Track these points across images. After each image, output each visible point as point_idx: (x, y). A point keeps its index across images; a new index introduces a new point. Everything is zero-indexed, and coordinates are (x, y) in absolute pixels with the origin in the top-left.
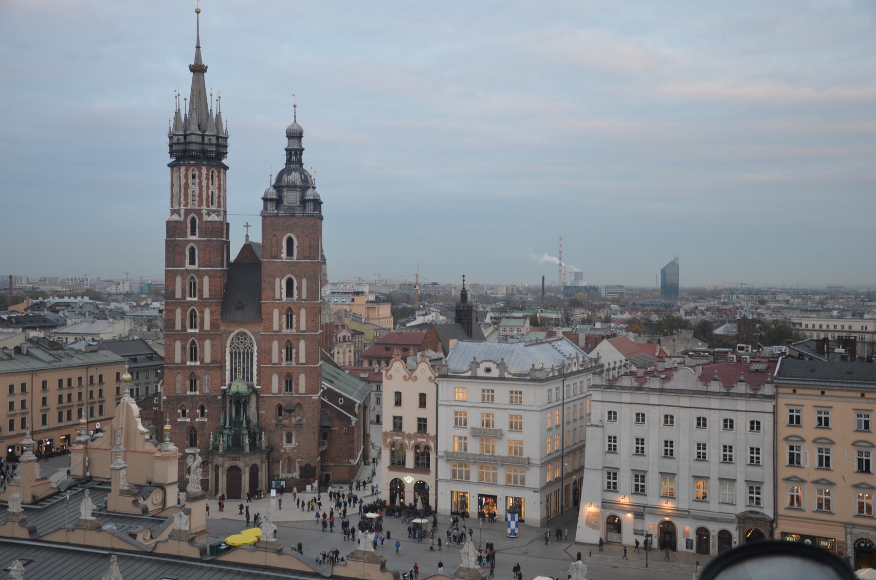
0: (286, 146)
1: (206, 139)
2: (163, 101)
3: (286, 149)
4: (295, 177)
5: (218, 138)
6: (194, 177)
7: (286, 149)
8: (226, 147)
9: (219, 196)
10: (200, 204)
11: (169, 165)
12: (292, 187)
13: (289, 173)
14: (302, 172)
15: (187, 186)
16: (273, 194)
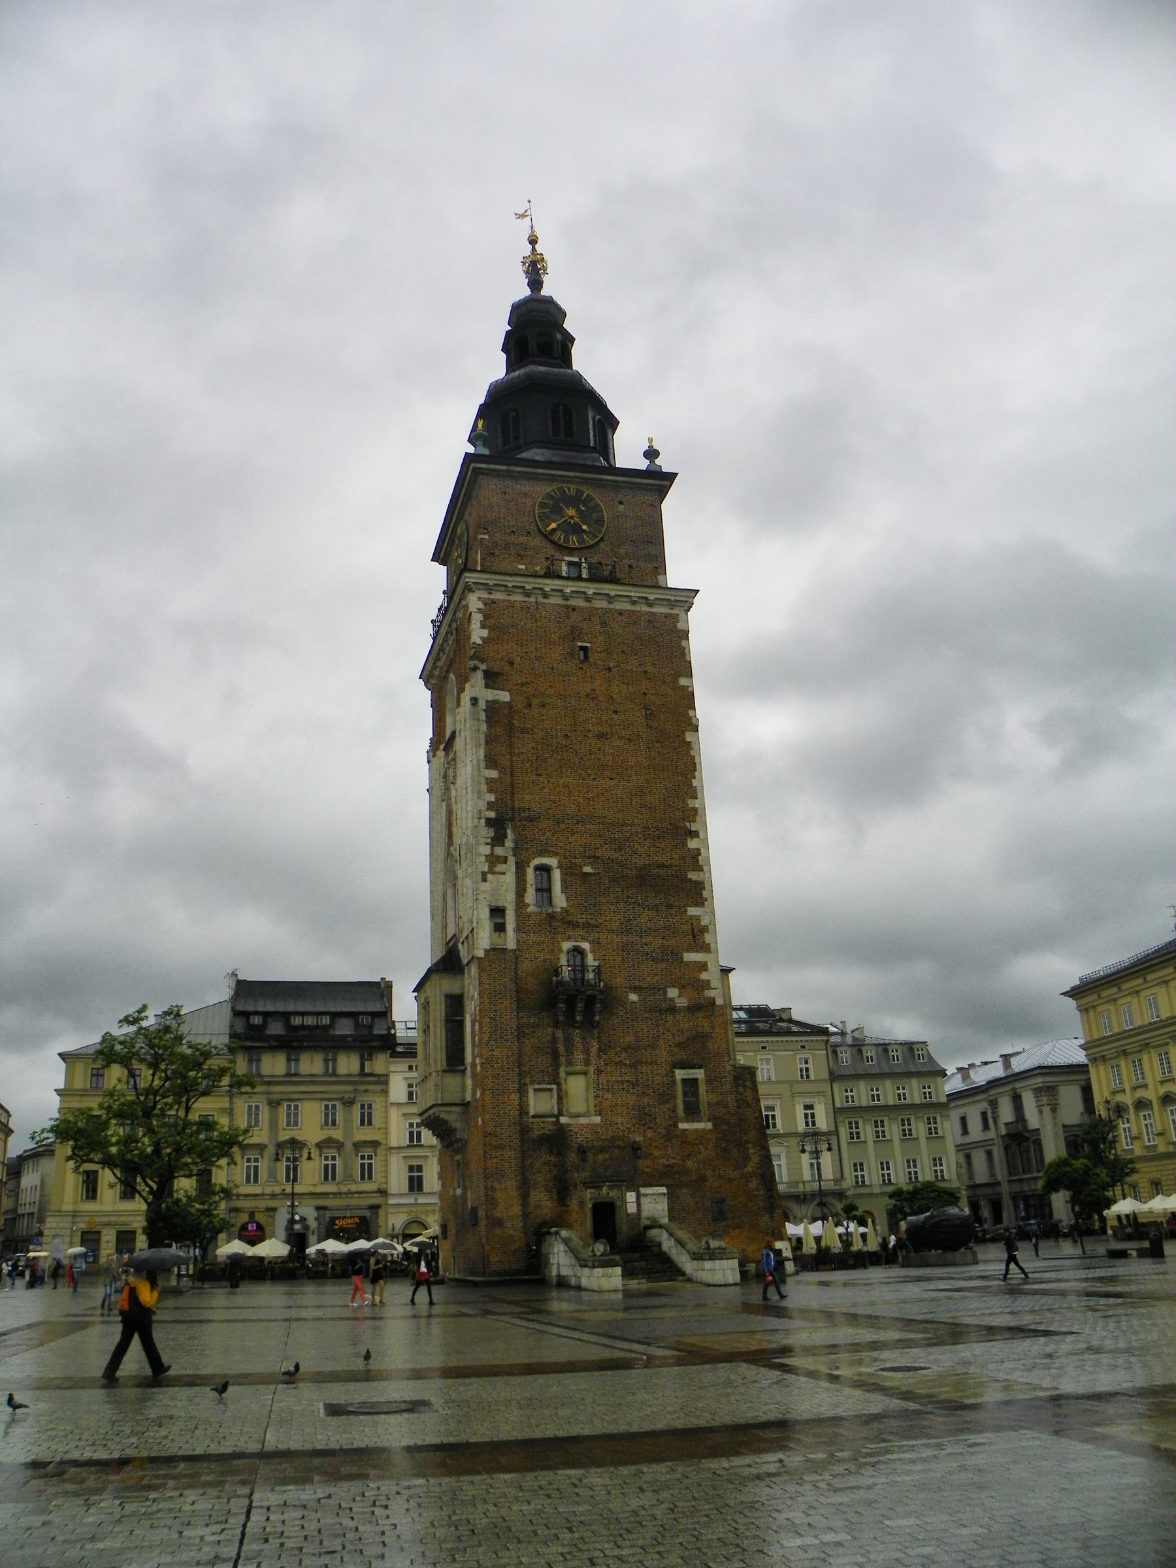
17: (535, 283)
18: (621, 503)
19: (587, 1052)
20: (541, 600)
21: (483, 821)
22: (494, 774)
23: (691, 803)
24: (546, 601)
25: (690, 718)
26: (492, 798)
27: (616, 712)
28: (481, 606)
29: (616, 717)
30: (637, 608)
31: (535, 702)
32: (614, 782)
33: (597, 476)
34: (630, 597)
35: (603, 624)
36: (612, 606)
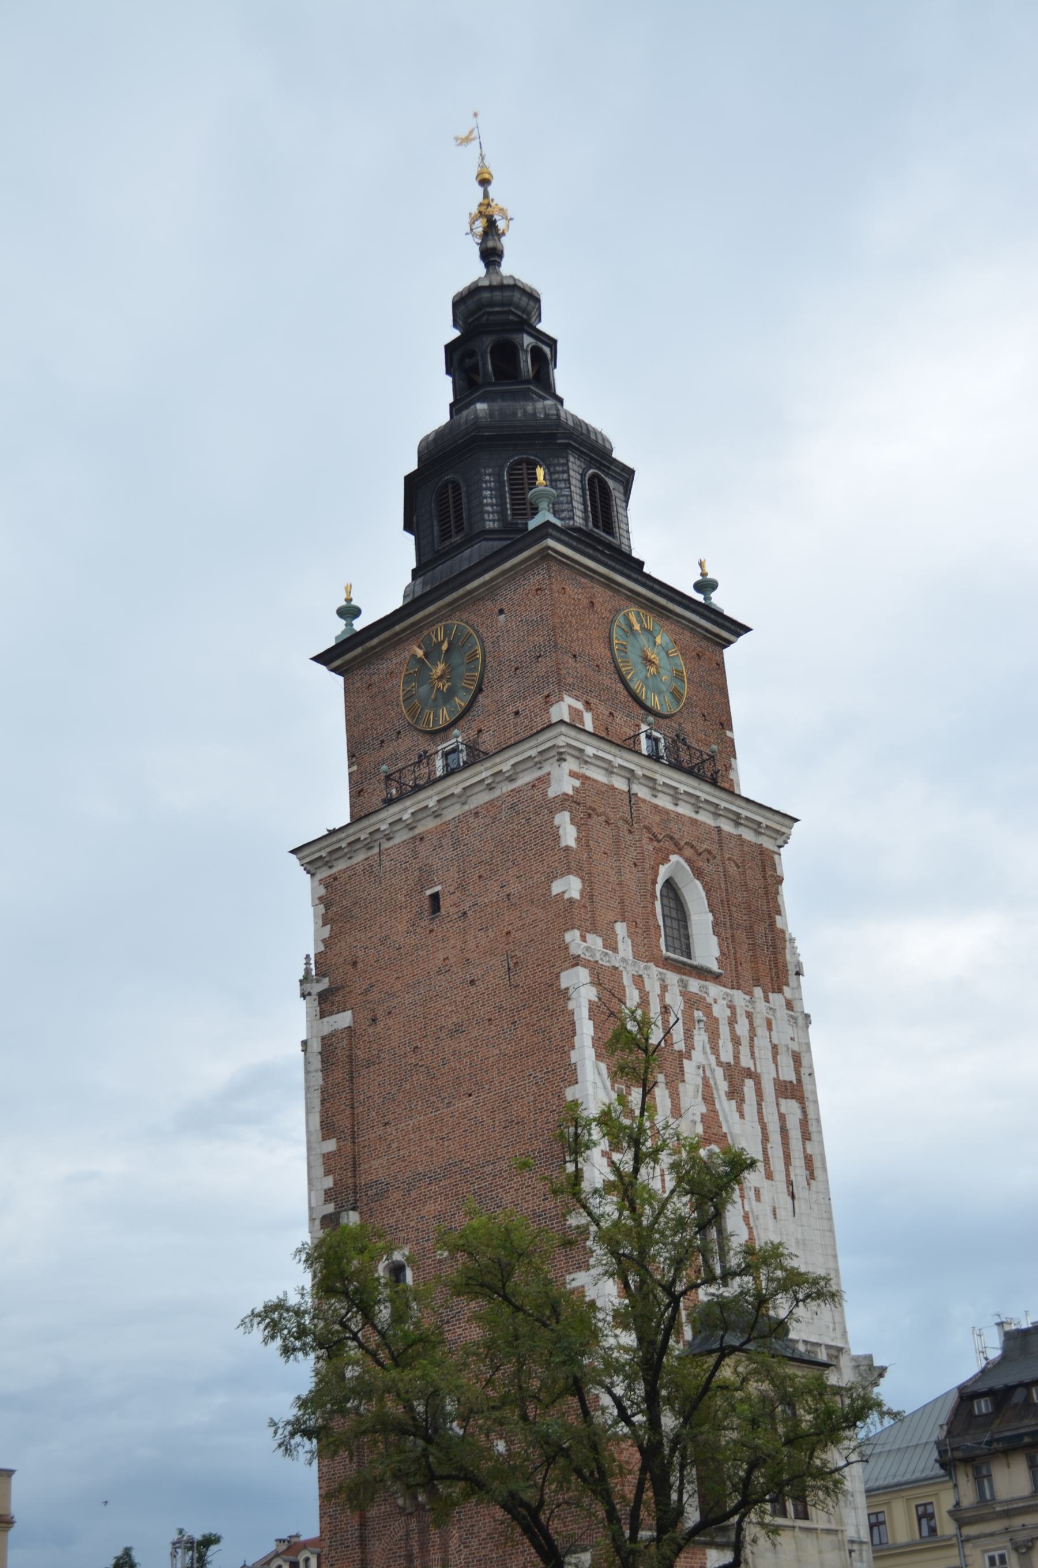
17: (491, 256)
18: (501, 612)
19: (444, 1547)
20: (386, 845)
21: (317, 1222)
22: (331, 1145)
23: (570, 1093)
24: (391, 844)
25: (567, 948)
26: (329, 1182)
27: (472, 982)
28: (322, 891)
29: (473, 989)
30: (496, 793)
31: (380, 1013)
32: (470, 1101)
33: (461, 592)
34: (483, 780)
35: (456, 844)
36: (466, 808)
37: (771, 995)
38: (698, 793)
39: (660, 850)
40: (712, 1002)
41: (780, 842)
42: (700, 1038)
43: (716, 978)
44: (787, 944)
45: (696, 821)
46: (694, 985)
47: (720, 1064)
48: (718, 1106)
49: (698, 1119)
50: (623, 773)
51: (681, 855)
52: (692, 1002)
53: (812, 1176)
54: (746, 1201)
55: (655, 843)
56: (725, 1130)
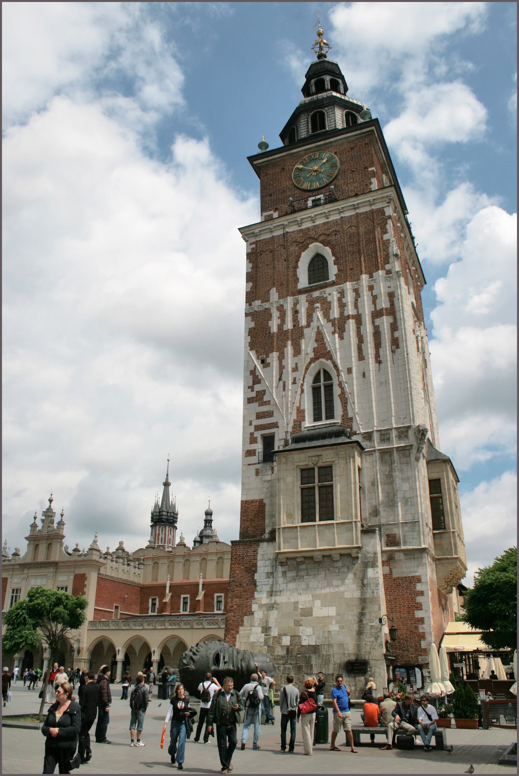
0: (205, 518)
1: (169, 514)
2: (149, 499)
3: (205, 520)
4: (208, 532)
5: (174, 514)
6: (162, 530)
7: (205, 520)
8: (177, 518)
9: (173, 541)
10: (165, 543)
11: (151, 526)
12: (208, 537)
13: (206, 530)
14: (212, 530)
15: (159, 534)
16: (199, 539)
37: (374, 274)
38: (324, 211)
39: (303, 246)
40: (328, 295)
41: (388, 201)
42: (319, 314)
43: (333, 284)
44: (391, 245)
45: (328, 222)
46: (316, 294)
47: (329, 320)
48: (325, 341)
49: (310, 350)
50: (279, 228)
51: (317, 242)
52: (311, 302)
53: (398, 347)
54: (340, 377)
55: (300, 245)
56: (328, 350)
